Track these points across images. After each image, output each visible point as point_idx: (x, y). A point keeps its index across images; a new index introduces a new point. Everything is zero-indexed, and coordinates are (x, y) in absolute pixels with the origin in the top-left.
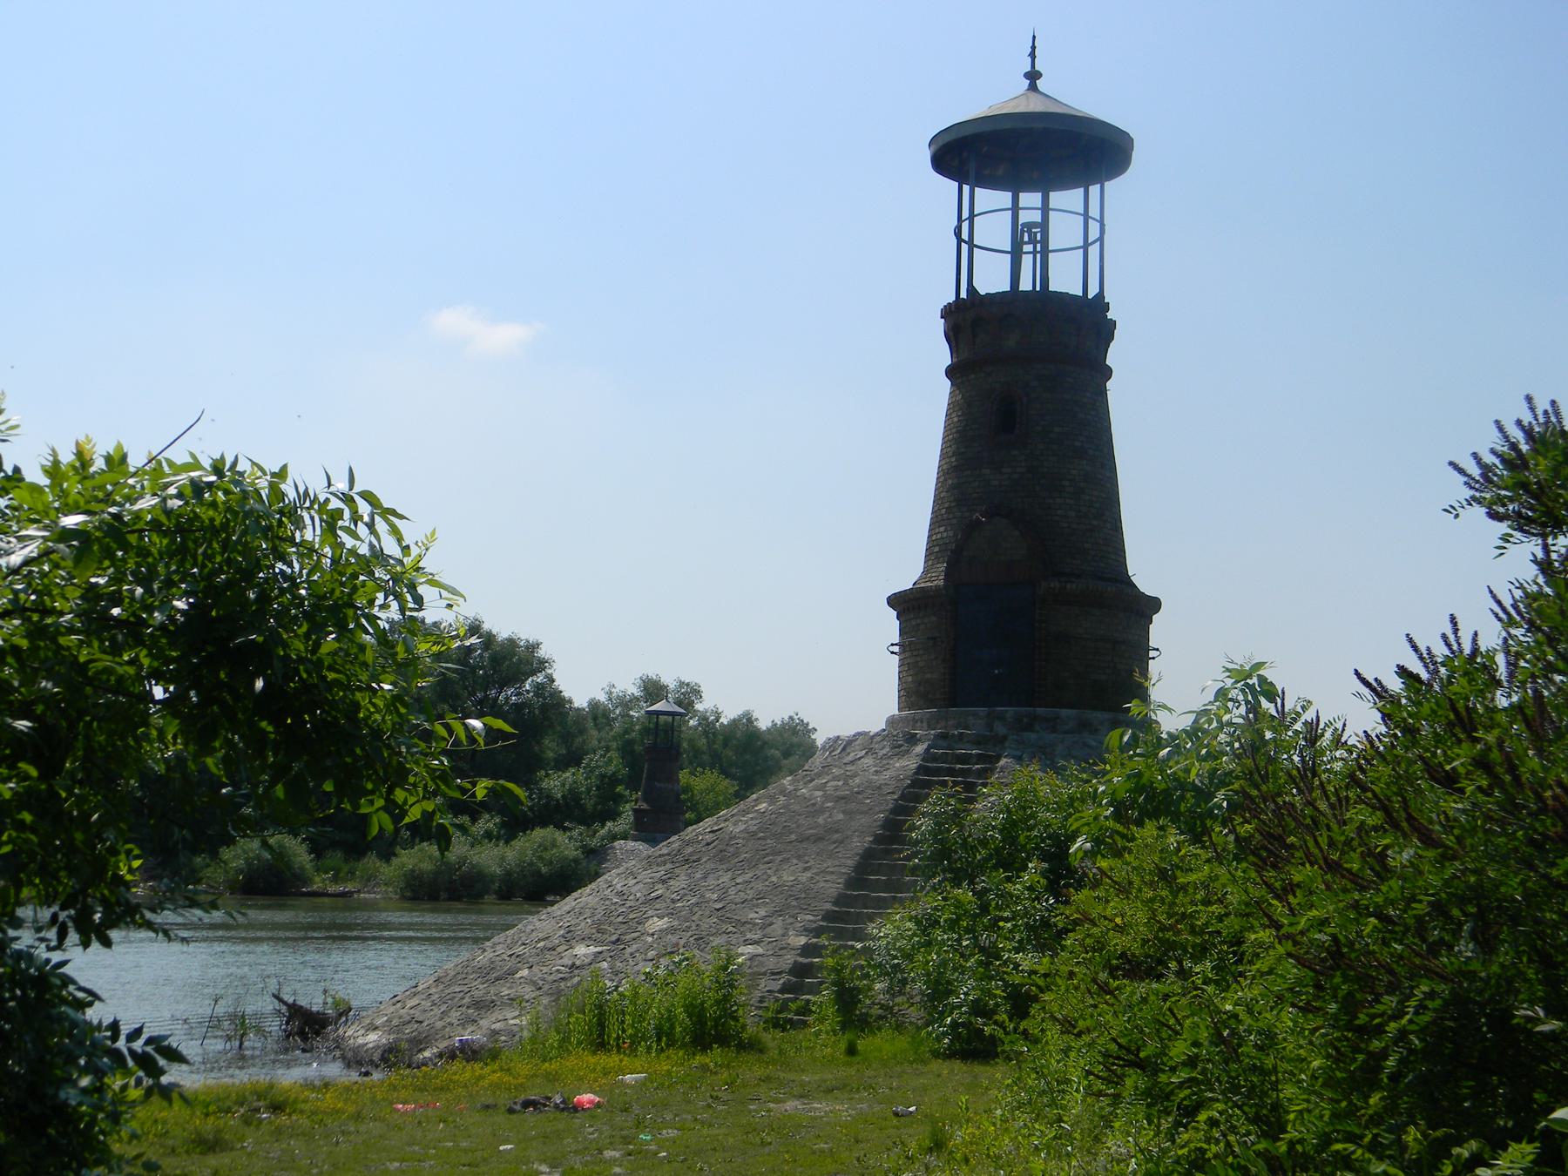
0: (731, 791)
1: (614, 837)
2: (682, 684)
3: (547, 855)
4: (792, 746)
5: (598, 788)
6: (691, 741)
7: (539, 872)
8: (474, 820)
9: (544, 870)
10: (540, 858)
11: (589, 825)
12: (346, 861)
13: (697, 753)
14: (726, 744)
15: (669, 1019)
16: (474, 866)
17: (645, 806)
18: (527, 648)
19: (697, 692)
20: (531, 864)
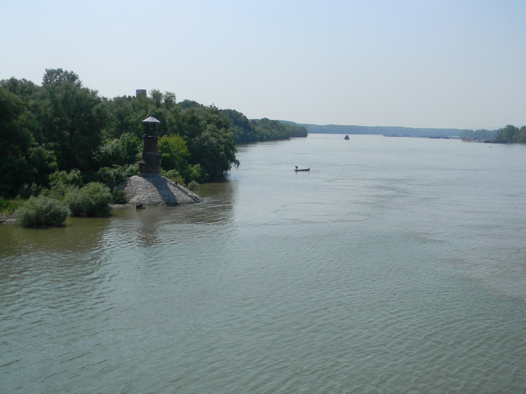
0: (184, 143)
1: (133, 173)
2: (168, 93)
3: (95, 196)
4: (211, 118)
5: (127, 149)
6: (170, 119)
7: (90, 204)
8: (68, 172)
9: (94, 203)
10: (92, 197)
11: (122, 165)
12: (6, 199)
13: (172, 124)
14: (183, 120)
15: (156, 241)
16: (56, 210)
17: (143, 162)
18: (92, 93)
19: (173, 96)
20: (88, 200)
